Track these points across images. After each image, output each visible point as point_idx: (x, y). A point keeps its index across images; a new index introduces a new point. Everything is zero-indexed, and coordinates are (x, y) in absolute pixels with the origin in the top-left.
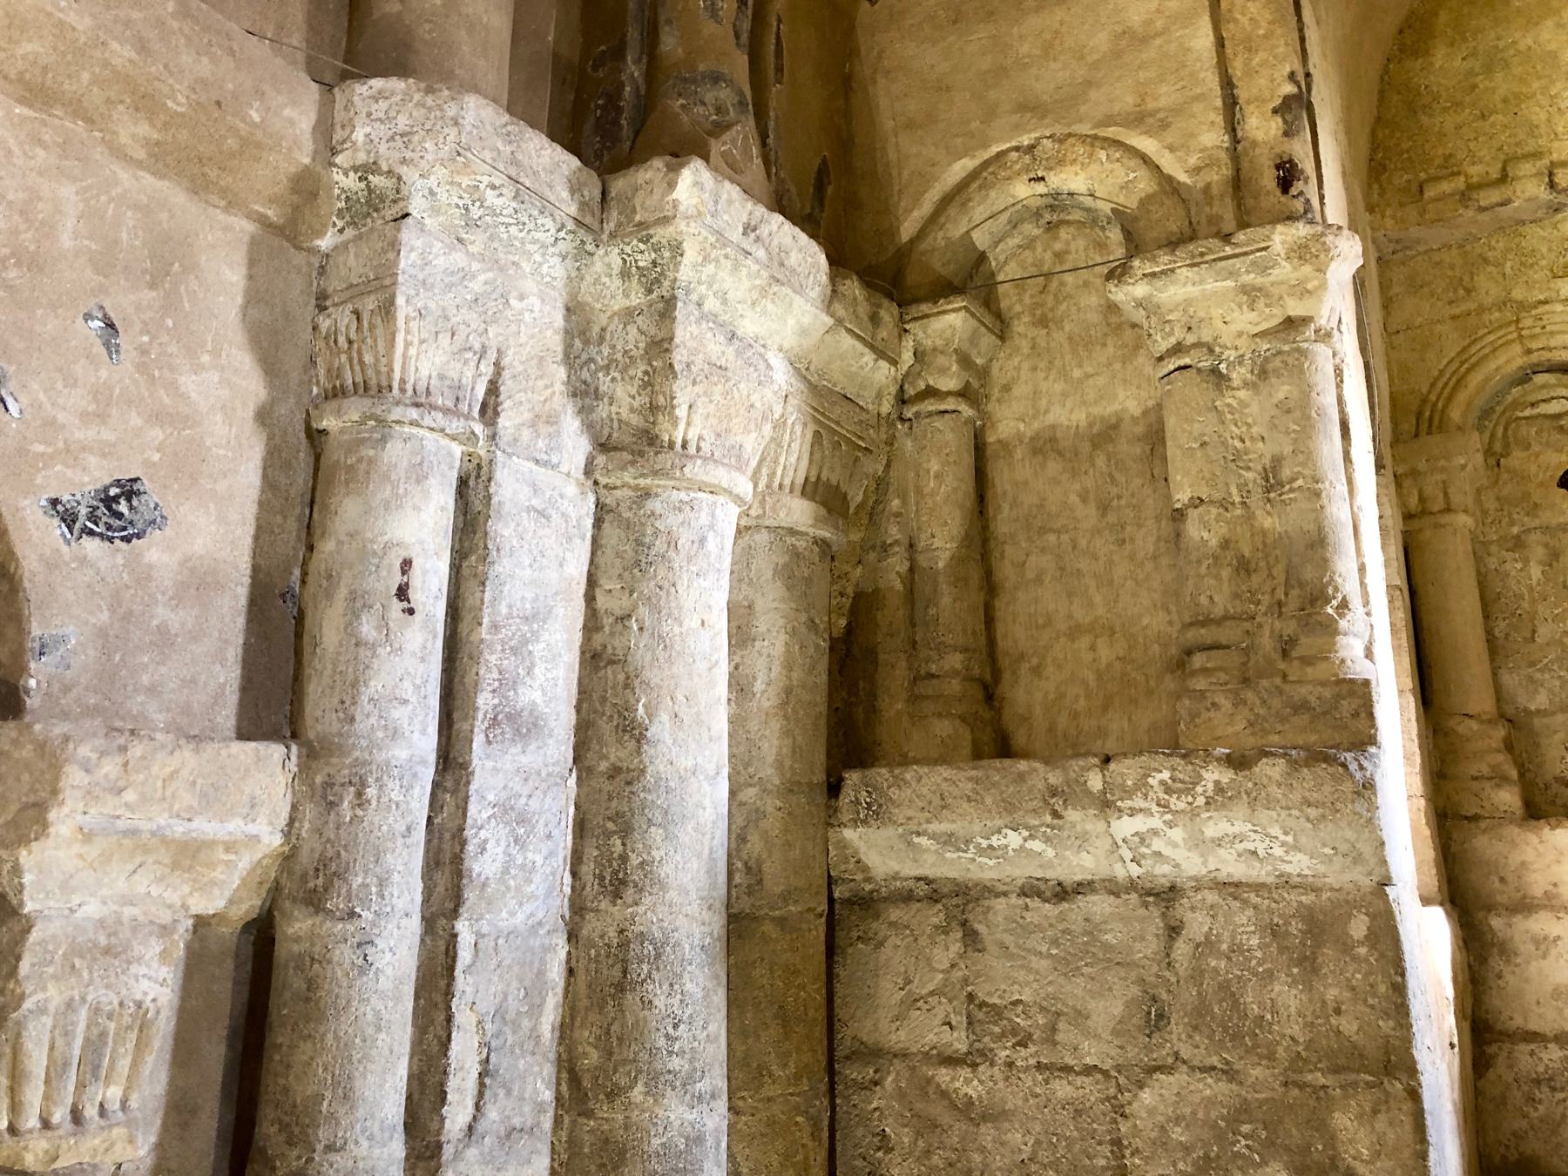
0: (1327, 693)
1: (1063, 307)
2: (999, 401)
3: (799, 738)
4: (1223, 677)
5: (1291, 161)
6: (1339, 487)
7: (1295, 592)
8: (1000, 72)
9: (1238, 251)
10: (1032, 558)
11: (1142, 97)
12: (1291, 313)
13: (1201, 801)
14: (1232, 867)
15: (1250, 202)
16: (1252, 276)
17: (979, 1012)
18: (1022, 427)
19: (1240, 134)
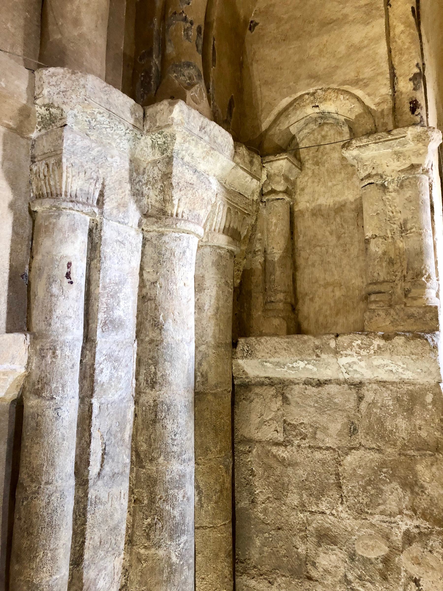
0: (421, 311)
1: (325, 157)
2: (299, 194)
3: (222, 327)
4: (382, 304)
5: (416, 100)
6: (429, 231)
7: (411, 272)
8: (301, 61)
9: (393, 137)
10: (311, 256)
11: (358, 73)
12: (413, 163)
13: (372, 352)
14: (383, 375)
15: (399, 117)
16: (399, 147)
18: (308, 205)
19: (396, 89)
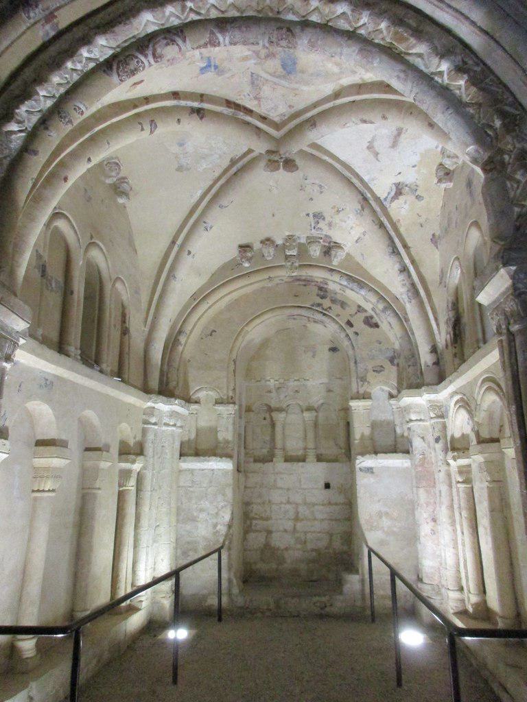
14: (219, 467)
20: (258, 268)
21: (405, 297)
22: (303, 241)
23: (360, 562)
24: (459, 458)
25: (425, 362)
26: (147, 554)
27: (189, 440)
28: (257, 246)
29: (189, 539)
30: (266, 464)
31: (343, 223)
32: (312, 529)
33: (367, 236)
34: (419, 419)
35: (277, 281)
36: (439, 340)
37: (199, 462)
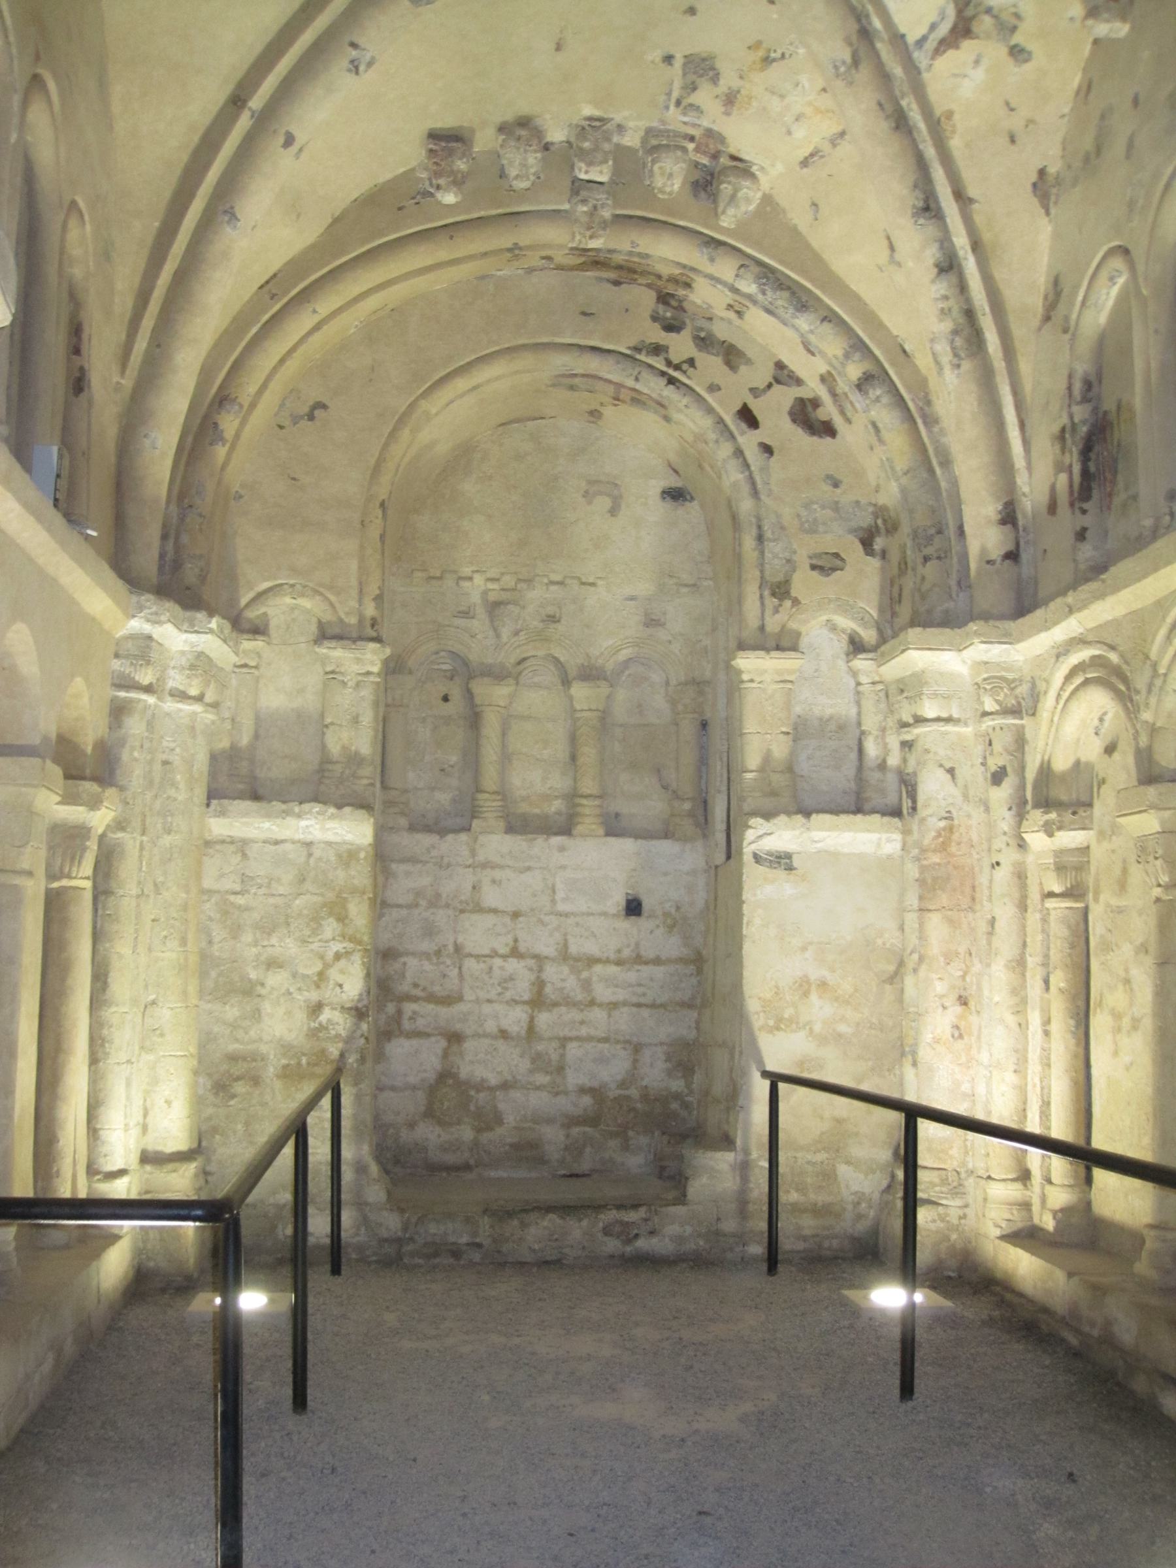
14: (330, 837)
17: (245, 878)
20: (482, 213)
21: (943, 349)
22: (632, 139)
23: (741, 1116)
24: (1060, 828)
25: (983, 550)
26: (128, 1084)
27: (233, 747)
28: (485, 140)
29: (233, 1047)
30: (450, 837)
31: (775, 101)
32: (584, 1031)
33: (845, 147)
34: (944, 715)
35: (534, 260)
36: (1026, 489)
37: (268, 816)
